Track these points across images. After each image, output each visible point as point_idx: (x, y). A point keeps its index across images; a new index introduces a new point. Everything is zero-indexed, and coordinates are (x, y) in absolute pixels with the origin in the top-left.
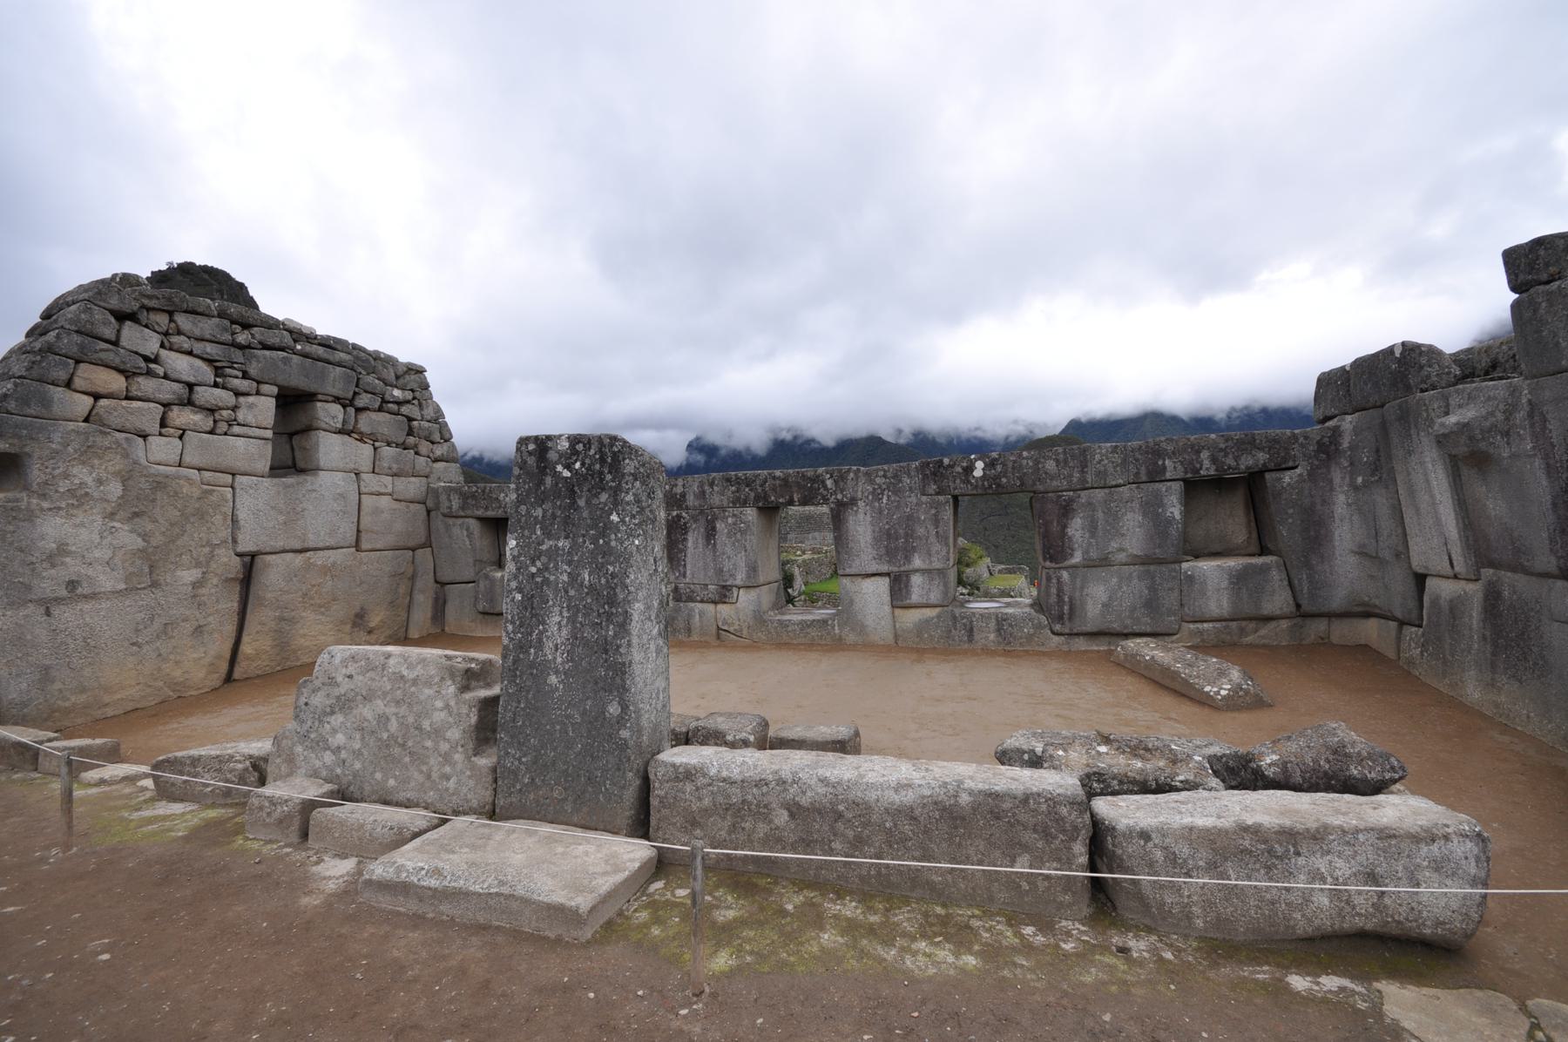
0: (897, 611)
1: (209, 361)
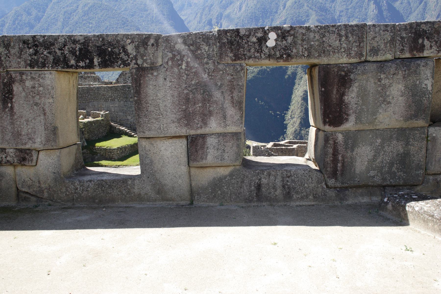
0: (193, 170)
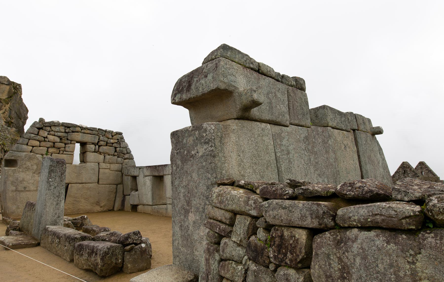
1: (59, 137)
